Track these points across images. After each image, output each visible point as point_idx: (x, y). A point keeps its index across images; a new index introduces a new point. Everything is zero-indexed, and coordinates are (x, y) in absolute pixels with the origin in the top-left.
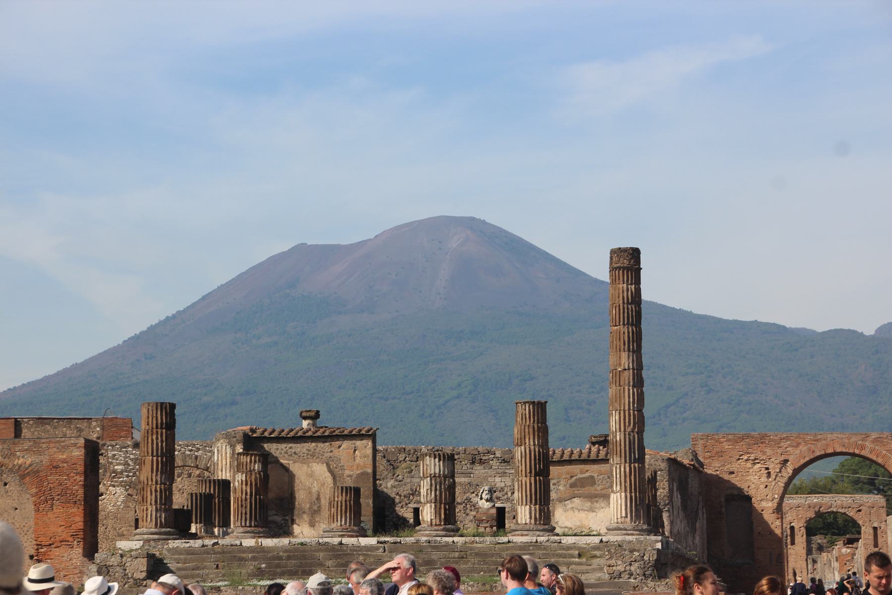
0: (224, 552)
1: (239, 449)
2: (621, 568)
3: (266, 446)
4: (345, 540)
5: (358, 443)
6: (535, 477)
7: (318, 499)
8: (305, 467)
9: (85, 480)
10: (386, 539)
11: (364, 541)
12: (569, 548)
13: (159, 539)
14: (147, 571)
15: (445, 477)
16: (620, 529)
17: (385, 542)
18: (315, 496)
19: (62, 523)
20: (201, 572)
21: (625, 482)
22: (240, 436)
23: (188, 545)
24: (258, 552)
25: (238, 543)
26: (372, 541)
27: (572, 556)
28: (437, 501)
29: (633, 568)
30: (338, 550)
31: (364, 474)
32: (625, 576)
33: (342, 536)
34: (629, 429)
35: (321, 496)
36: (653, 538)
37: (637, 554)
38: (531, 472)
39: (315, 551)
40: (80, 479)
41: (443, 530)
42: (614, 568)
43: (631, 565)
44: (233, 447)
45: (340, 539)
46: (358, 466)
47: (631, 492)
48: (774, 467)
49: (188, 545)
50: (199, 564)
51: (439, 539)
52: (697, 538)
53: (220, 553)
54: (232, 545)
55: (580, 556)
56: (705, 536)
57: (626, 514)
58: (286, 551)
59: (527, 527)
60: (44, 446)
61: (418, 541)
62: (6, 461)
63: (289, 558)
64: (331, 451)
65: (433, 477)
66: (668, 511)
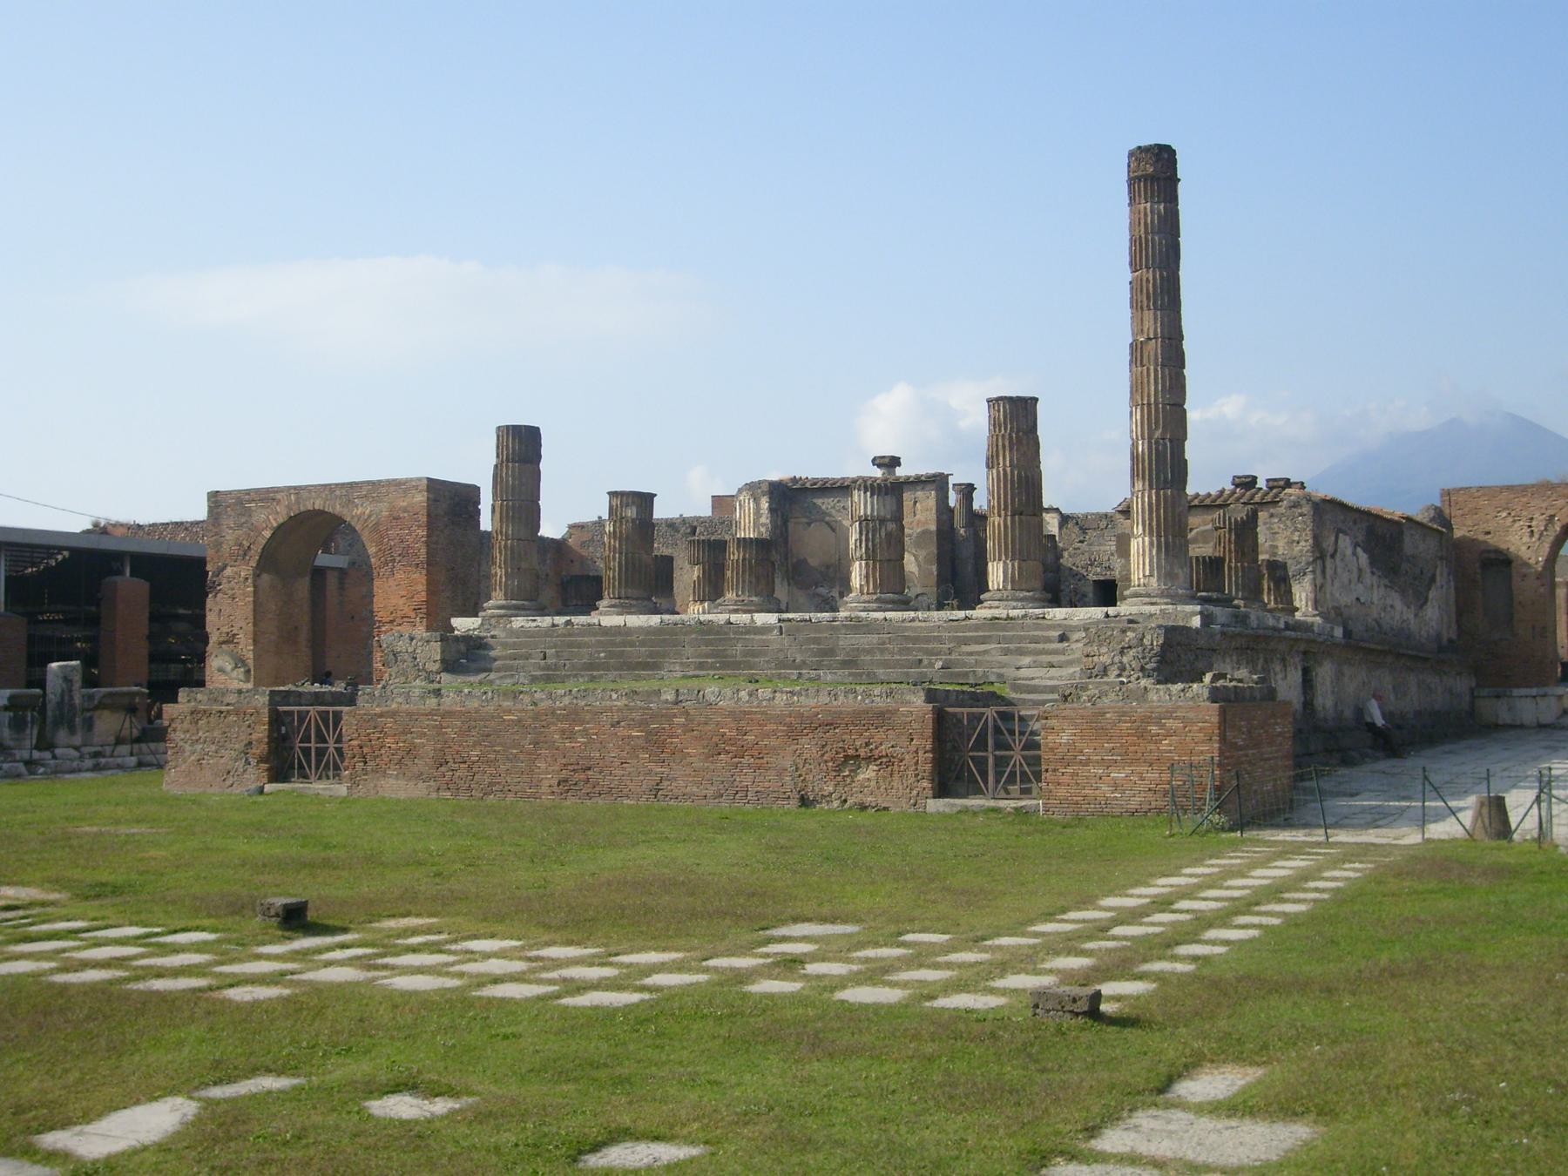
1: (765, 504)
2: (1106, 659)
3: (819, 502)
4: (734, 618)
5: (919, 494)
6: (1013, 515)
9: (428, 536)
10: (791, 616)
11: (762, 619)
12: (1050, 628)
14: (443, 661)
15: (882, 521)
16: (1141, 596)
17: (789, 620)
21: (1151, 519)
22: (765, 488)
26: (771, 618)
27: (1048, 640)
28: (870, 556)
29: (1125, 660)
31: (925, 532)
32: (1113, 672)
33: (736, 611)
34: (1158, 434)
36: (1189, 608)
38: (1006, 509)
40: (422, 532)
41: (877, 600)
43: (1122, 653)
44: (757, 501)
46: (919, 522)
47: (1159, 536)
48: (1539, 523)
51: (863, 614)
52: (1432, 612)
55: (1063, 638)
56: (1453, 609)
57: (1151, 570)
63: (643, 643)
65: (864, 521)
66: (1313, 572)
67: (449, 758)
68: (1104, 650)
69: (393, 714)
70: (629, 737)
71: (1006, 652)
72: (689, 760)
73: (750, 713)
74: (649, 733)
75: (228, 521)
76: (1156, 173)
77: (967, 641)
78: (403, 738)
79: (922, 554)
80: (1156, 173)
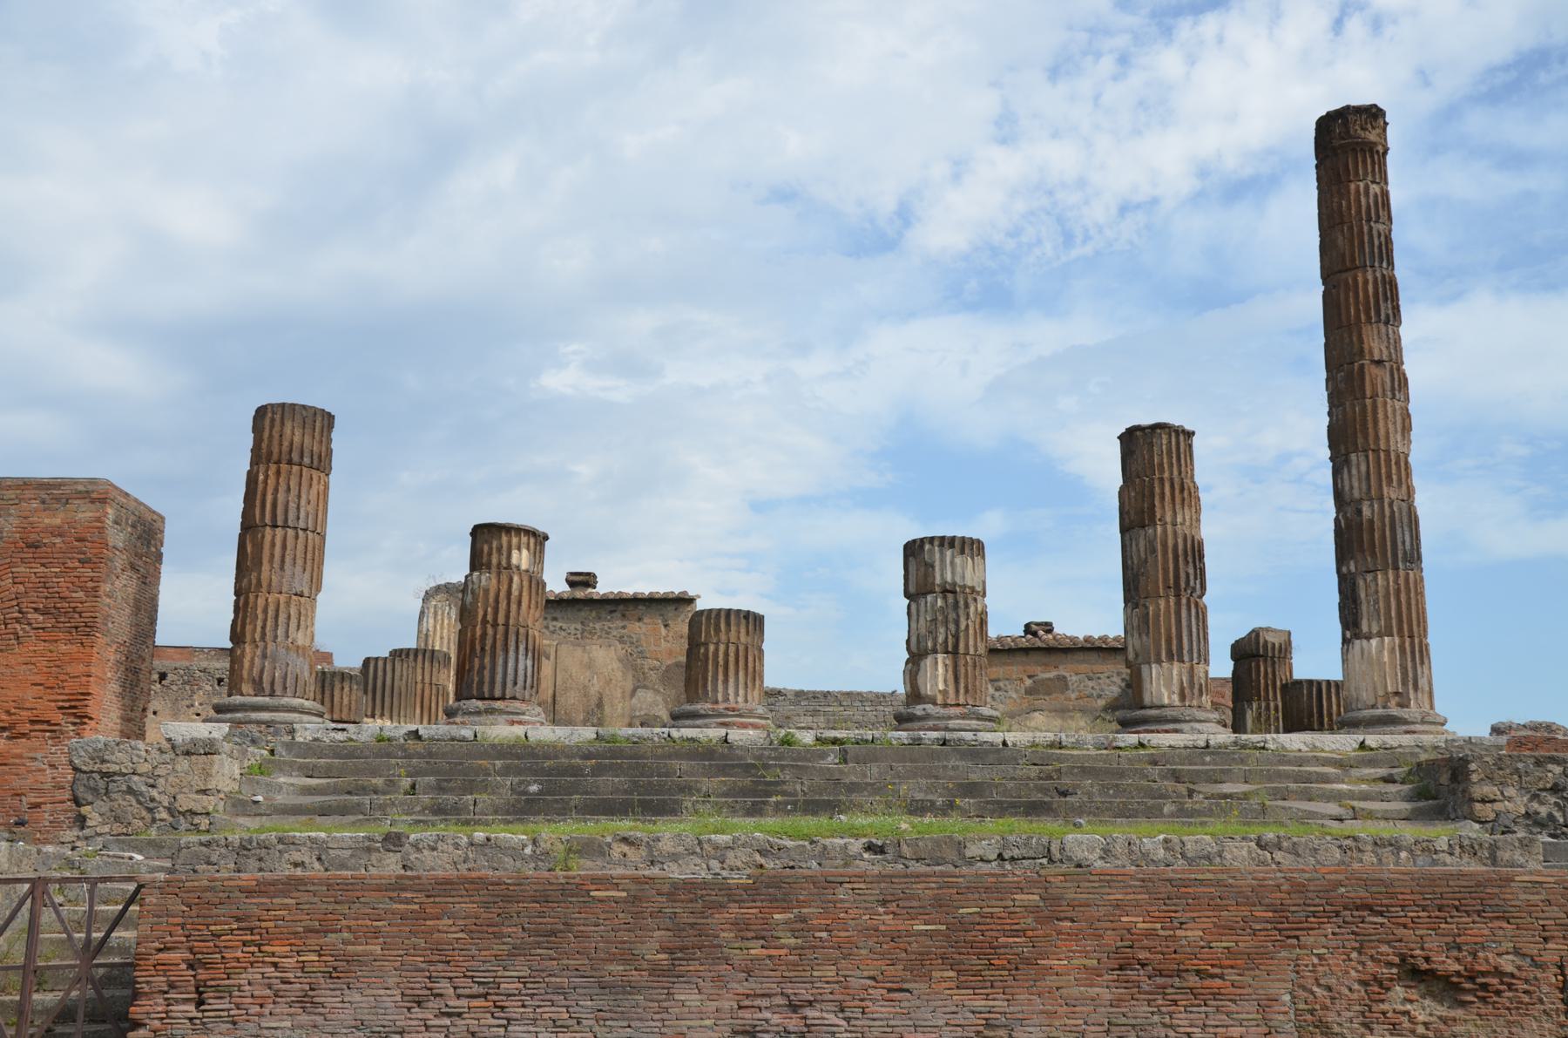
0: (431, 755)
7: (600, 705)
8: (579, 651)
13: (269, 724)
18: (594, 701)
19: (38, 679)
20: (366, 800)
23: (340, 736)
24: (518, 757)
25: (467, 733)
27: (1325, 779)
30: (723, 756)
31: (677, 665)
35: (605, 700)
37: (1558, 769)
39: (663, 757)
42: (1498, 806)
45: (722, 732)
49: (340, 736)
50: (363, 780)
53: (420, 756)
54: (453, 739)
58: (587, 757)
59: (1168, 713)
60: (10, 494)
61: (917, 742)
64: (624, 627)
67: (444, 986)
68: (1510, 791)
69: (293, 885)
70: (909, 934)
72: (1051, 981)
73: (1185, 883)
74: (963, 925)
76: (1347, 145)
78: (313, 941)
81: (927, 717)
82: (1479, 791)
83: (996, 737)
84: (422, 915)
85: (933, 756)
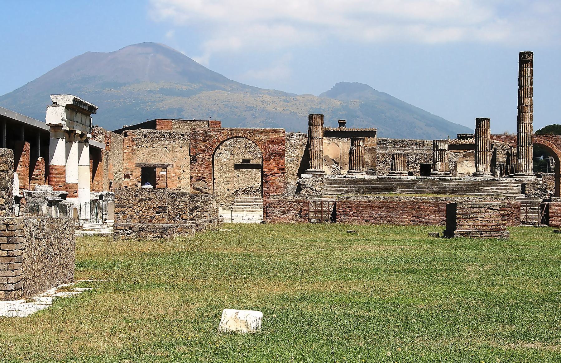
59: (481, 173)
62: (251, 138)
69: (355, 202)
71: (497, 189)
75: (200, 138)
77: (482, 186)
79: (372, 155)
80: (525, 59)
81: (436, 174)
82: (526, 189)
83: (449, 178)
84: (371, 206)
85: (438, 181)
